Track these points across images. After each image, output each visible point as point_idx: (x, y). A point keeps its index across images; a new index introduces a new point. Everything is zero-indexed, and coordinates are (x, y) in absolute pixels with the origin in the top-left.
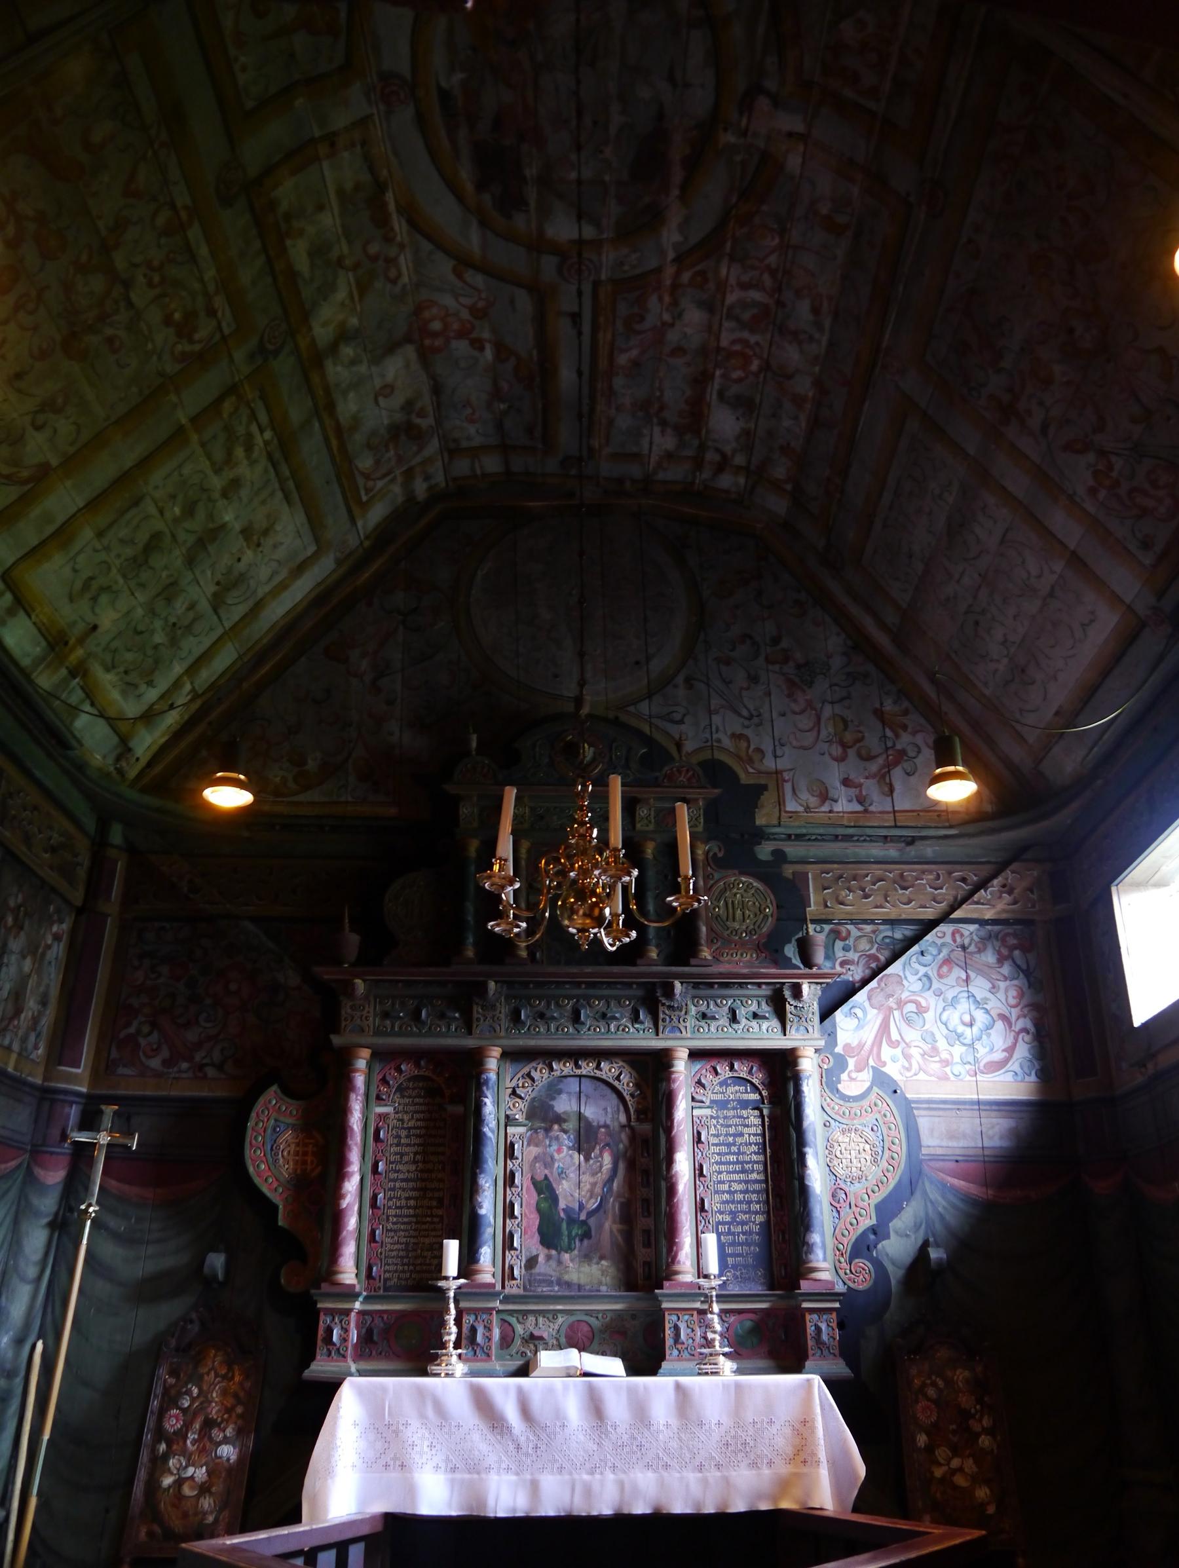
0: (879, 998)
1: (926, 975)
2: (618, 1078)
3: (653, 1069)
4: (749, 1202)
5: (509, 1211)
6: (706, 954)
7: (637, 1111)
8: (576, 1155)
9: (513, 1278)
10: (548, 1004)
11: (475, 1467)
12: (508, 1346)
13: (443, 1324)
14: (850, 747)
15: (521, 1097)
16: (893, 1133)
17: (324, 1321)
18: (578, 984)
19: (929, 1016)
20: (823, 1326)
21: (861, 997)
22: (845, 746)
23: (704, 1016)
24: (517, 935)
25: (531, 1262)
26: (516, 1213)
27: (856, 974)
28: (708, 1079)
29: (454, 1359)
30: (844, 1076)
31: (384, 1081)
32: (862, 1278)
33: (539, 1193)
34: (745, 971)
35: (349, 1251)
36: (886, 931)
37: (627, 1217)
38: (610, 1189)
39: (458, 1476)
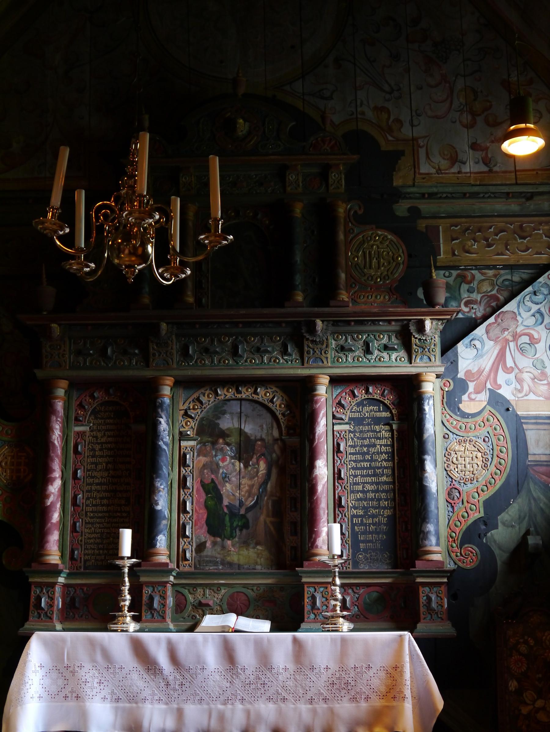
0: (495, 331)
1: (539, 311)
2: (272, 401)
3: (301, 394)
4: (379, 500)
5: (182, 508)
6: (344, 296)
7: (288, 428)
8: (237, 463)
9: (185, 559)
10: (212, 341)
11: (134, 699)
12: (182, 611)
13: (120, 593)
14: (479, 115)
15: (191, 417)
16: (501, 443)
17: (35, 591)
18: (236, 324)
19: (541, 346)
20: (433, 597)
21: (480, 331)
22: (474, 115)
23: (342, 349)
24: (87, 273)
25: (201, 547)
26: (188, 508)
27: (479, 311)
28: (347, 400)
29: (128, 619)
30: (465, 397)
31: (81, 406)
32: (471, 558)
33: (207, 493)
34: (376, 310)
35: (54, 537)
36: (505, 275)
37: (278, 511)
38: (265, 489)
39: (120, 705)
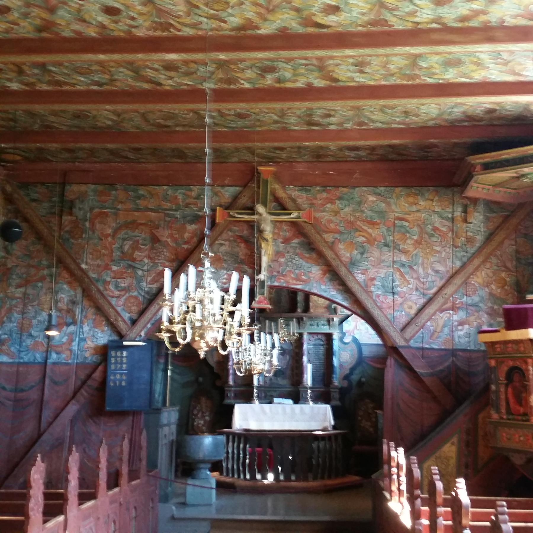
17: (226, 392)
30: (345, 337)
32: (345, 384)
37: (292, 370)
